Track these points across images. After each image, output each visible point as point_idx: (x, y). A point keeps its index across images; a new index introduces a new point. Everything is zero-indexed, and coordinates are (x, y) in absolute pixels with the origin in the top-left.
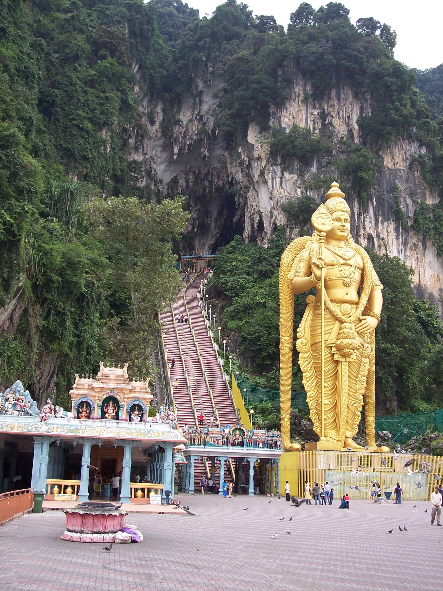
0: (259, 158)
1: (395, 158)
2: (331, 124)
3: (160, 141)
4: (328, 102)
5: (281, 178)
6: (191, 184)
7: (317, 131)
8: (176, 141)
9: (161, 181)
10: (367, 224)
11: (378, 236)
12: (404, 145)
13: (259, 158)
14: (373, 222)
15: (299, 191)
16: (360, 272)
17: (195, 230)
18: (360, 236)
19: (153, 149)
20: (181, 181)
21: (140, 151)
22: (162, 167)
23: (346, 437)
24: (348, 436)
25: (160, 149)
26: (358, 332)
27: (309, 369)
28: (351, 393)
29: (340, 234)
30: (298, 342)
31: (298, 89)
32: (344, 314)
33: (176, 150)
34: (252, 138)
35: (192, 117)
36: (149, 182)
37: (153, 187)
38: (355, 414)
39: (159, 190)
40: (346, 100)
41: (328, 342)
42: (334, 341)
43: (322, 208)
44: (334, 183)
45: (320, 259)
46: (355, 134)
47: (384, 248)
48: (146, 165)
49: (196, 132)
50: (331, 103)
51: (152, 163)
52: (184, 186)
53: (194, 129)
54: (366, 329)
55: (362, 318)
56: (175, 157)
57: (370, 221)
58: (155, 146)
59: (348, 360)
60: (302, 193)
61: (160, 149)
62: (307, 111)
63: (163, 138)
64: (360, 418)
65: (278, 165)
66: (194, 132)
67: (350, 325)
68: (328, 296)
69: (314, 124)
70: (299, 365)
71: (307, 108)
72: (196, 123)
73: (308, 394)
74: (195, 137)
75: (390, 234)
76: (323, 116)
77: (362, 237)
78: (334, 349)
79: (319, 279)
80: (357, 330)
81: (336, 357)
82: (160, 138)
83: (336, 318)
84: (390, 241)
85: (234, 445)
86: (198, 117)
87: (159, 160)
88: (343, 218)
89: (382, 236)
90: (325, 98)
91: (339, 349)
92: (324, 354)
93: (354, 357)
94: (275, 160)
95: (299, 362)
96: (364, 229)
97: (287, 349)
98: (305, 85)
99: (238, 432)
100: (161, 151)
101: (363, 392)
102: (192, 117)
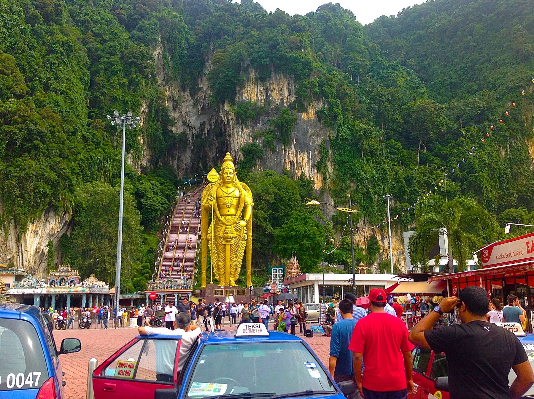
0: (232, 119)
1: (309, 113)
2: (271, 95)
3: (191, 102)
4: (269, 81)
5: (242, 132)
6: (213, 127)
7: (263, 101)
8: (199, 101)
10: (291, 155)
11: (297, 162)
13: (232, 119)
14: (295, 154)
15: (251, 139)
16: (238, 199)
17: (217, 155)
18: (286, 163)
19: (187, 108)
21: (178, 110)
22: (194, 118)
25: (191, 107)
29: (227, 180)
30: (208, 235)
31: (252, 75)
32: (227, 221)
33: (200, 108)
34: (226, 108)
36: (186, 128)
37: (188, 132)
38: (236, 269)
40: (280, 79)
43: (213, 170)
44: (228, 153)
45: (211, 196)
46: (285, 101)
47: (300, 168)
48: (182, 119)
50: (272, 82)
52: (209, 129)
55: (237, 222)
56: (200, 112)
57: (293, 153)
58: (188, 106)
59: (229, 243)
60: (253, 140)
61: (191, 107)
62: (257, 88)
63: (192, 100)
64: (240, 271)
65: (240, 124)
67: (229, 227)
68: (219, 212)
69: (261, 96)
70: (208, 247)
71: (257, 87)
75: (304, 160)
76: (267, 90)
77: (287, 163)
78: (222, 239)
79: (211, 206)
81: (224, 242)
82: (190, 101)
83: (224, 224)
84: (304, 164)
85: (167, 288)
88: (228, 172)
89: (299, 162)
90: (268, 79)
91: (225, 238)
92: (219, 241)
93: (233, 242)
94: (238, 121)
96: (289, 158)
97: (204, 239)
98: (256, 72)
99: (170, 282)
101: (242, 258)
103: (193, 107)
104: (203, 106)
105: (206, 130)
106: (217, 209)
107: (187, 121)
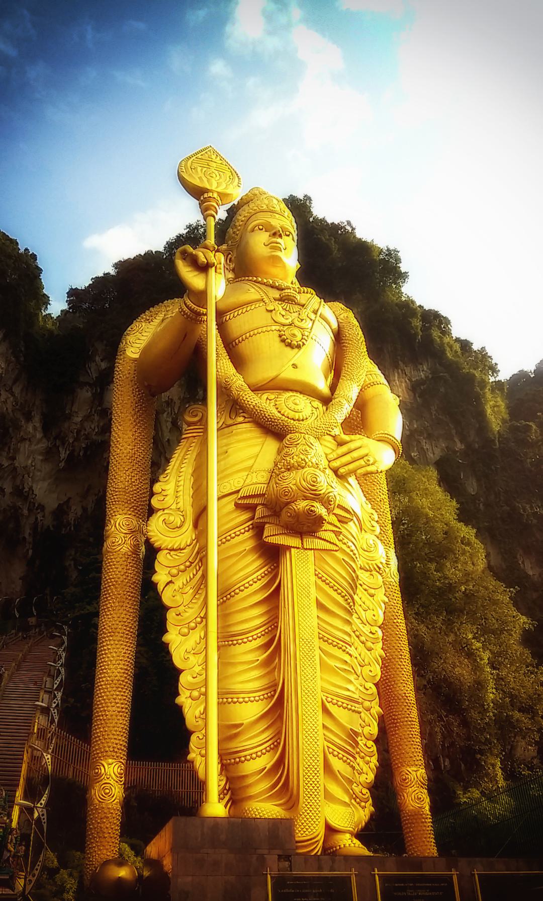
3: (40, 445)
9: (42, 507)
12: (407, 370)
19: (28, 457)
20: (73, 508)
21: (5, 454)
22: (45, 485)
23: (330, 830)
24: (335, 823)
25: (40, 458)
26: (335, 471)
27: (188, 597)
28: (332, 663)
33: (63, 454)
35: (91, 411)
39: (37, 518)
41: (241, 494)
42: (260, 488)
48: (14, 478)
49: (96, 431)
51: (26, 476)
52: (79, 513)
53: (93, 427)
54: (362, 462)
56: (62, 464)
61: (40, 458)
63: (44, 440)
64: (374, 761)
66: (94, 430)
70: (155, 585)
72: (96, 418)
73: (185, 679)
74: (94, 437)
78: (260, 511)
80: (335, 464)
86: (100, 408)
87: (39, 473)
95: (155, 578)
97: (126, 548)
100: (42, 460)
102: (91, 411)
103: (45, 460)
104: (70, 457)
105: (71, 517)
106: (223, 352)
107: (26, 485)
